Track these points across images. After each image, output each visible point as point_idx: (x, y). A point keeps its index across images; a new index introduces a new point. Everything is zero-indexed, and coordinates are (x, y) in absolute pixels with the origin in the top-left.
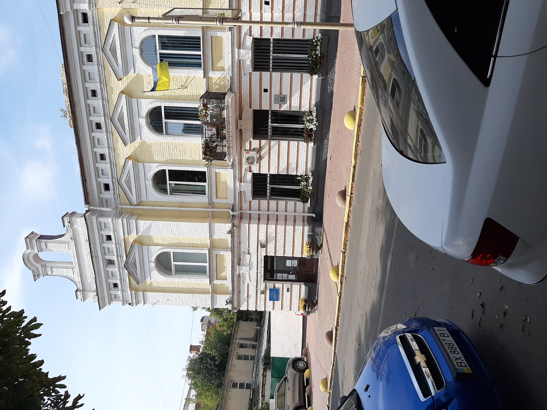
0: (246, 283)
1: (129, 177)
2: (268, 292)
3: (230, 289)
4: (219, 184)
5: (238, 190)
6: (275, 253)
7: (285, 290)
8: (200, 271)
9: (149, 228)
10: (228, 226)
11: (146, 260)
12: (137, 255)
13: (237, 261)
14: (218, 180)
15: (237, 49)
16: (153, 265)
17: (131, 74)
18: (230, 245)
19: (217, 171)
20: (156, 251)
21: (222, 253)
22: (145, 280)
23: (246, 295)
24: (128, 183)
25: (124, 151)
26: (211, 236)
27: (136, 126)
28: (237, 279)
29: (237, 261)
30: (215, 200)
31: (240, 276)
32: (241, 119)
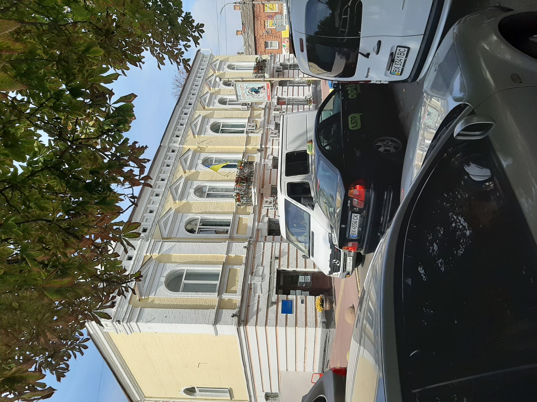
0: (257, 295)
1: (168, 221)
2: (280, 304)
3: (238, 304)
4: (240, 225)
5: (256, 228)
6: (286, 316)
7: (299, 301)
8: (210, 289)
9: (171, 248)
10: (246, 244)
11: (158, 275)
12: (151, 269)
13: (250, 271)
14: (240, 222)
15: (263, 160)
16: (163, 279)
17: (193, 171)
18: (244, 262)
19: (241, 216)
20: (170, 268)
21: (235, 267)
22: (149, 295)
23: (255, 309)
24: (166, 224)
25: (171, 205)
26: (228, 253)
27: (186, 193)
28: (247, 291)
29: (250, 271)
30: (235, 235)
31: (251, 289)
32: (263, 187)
